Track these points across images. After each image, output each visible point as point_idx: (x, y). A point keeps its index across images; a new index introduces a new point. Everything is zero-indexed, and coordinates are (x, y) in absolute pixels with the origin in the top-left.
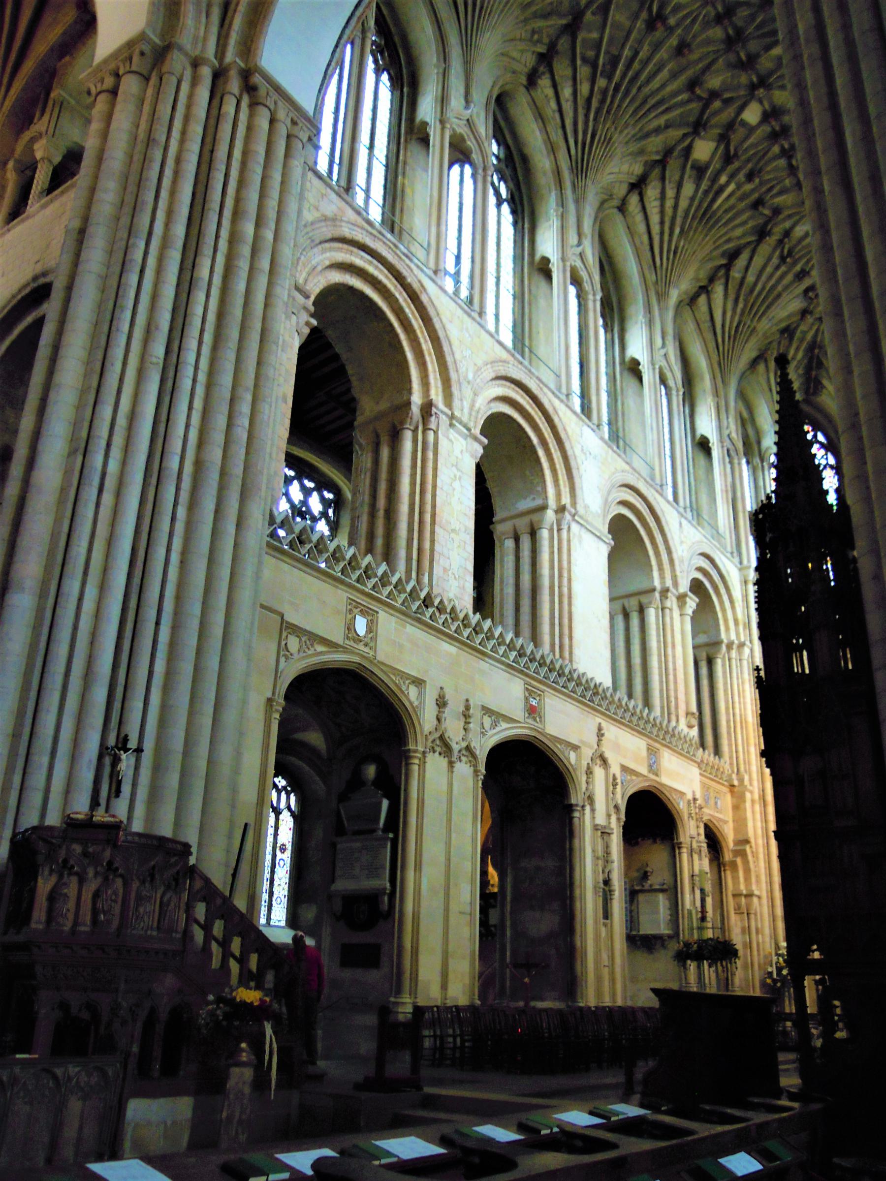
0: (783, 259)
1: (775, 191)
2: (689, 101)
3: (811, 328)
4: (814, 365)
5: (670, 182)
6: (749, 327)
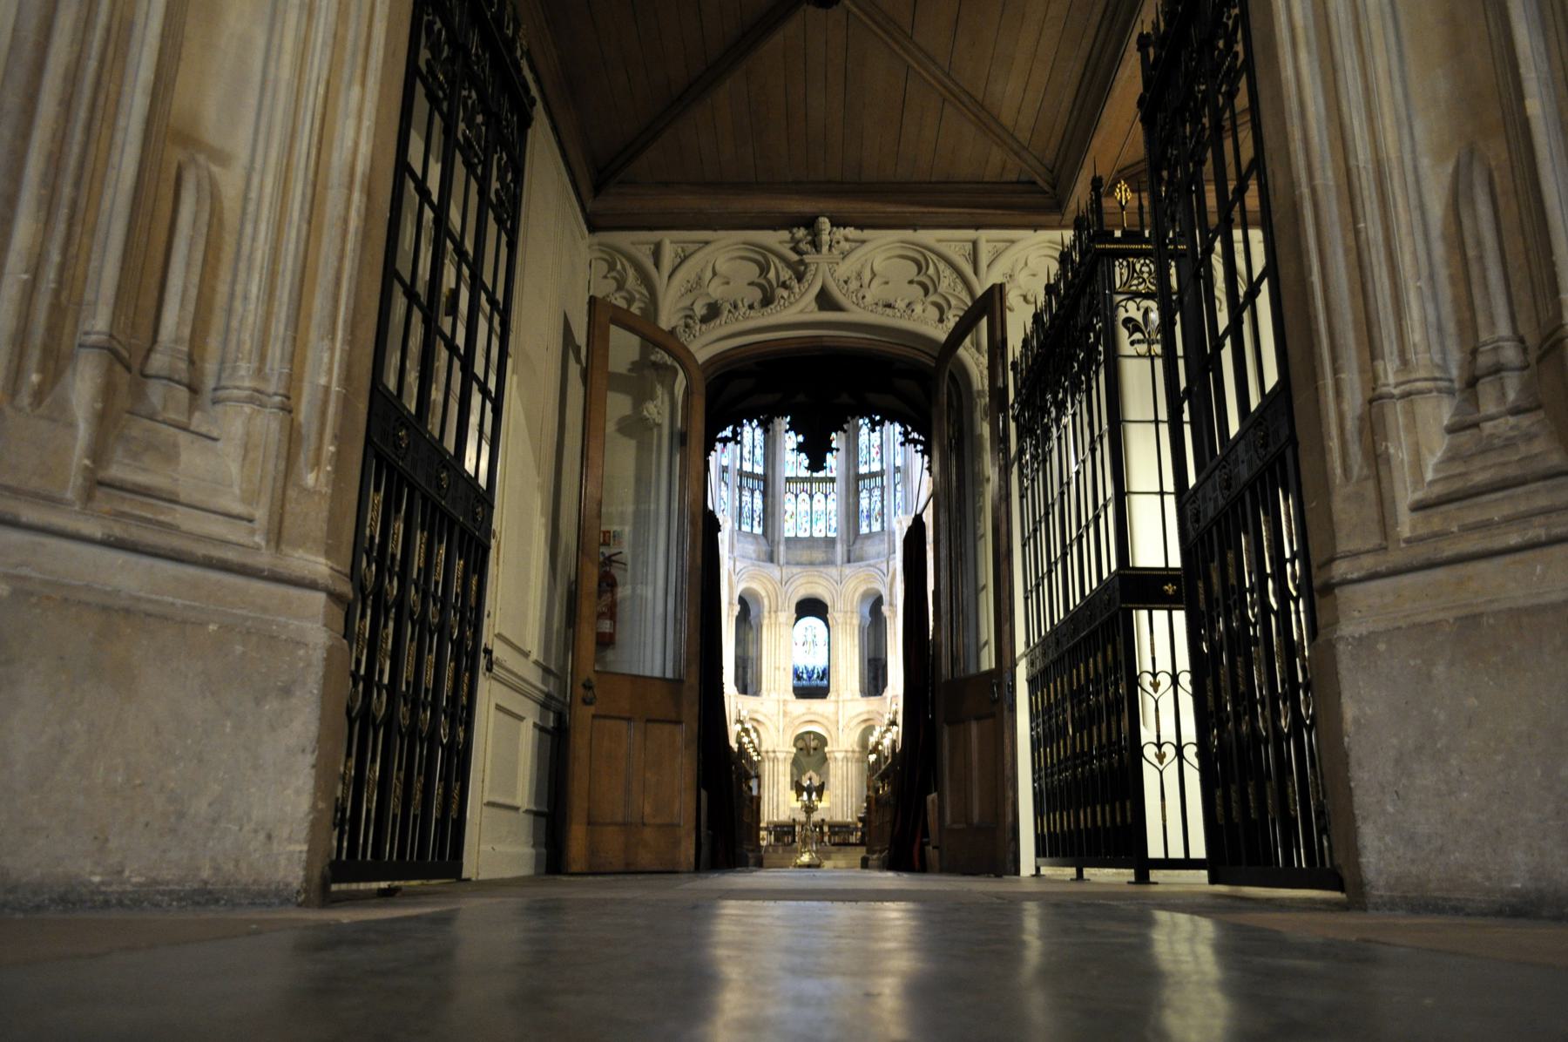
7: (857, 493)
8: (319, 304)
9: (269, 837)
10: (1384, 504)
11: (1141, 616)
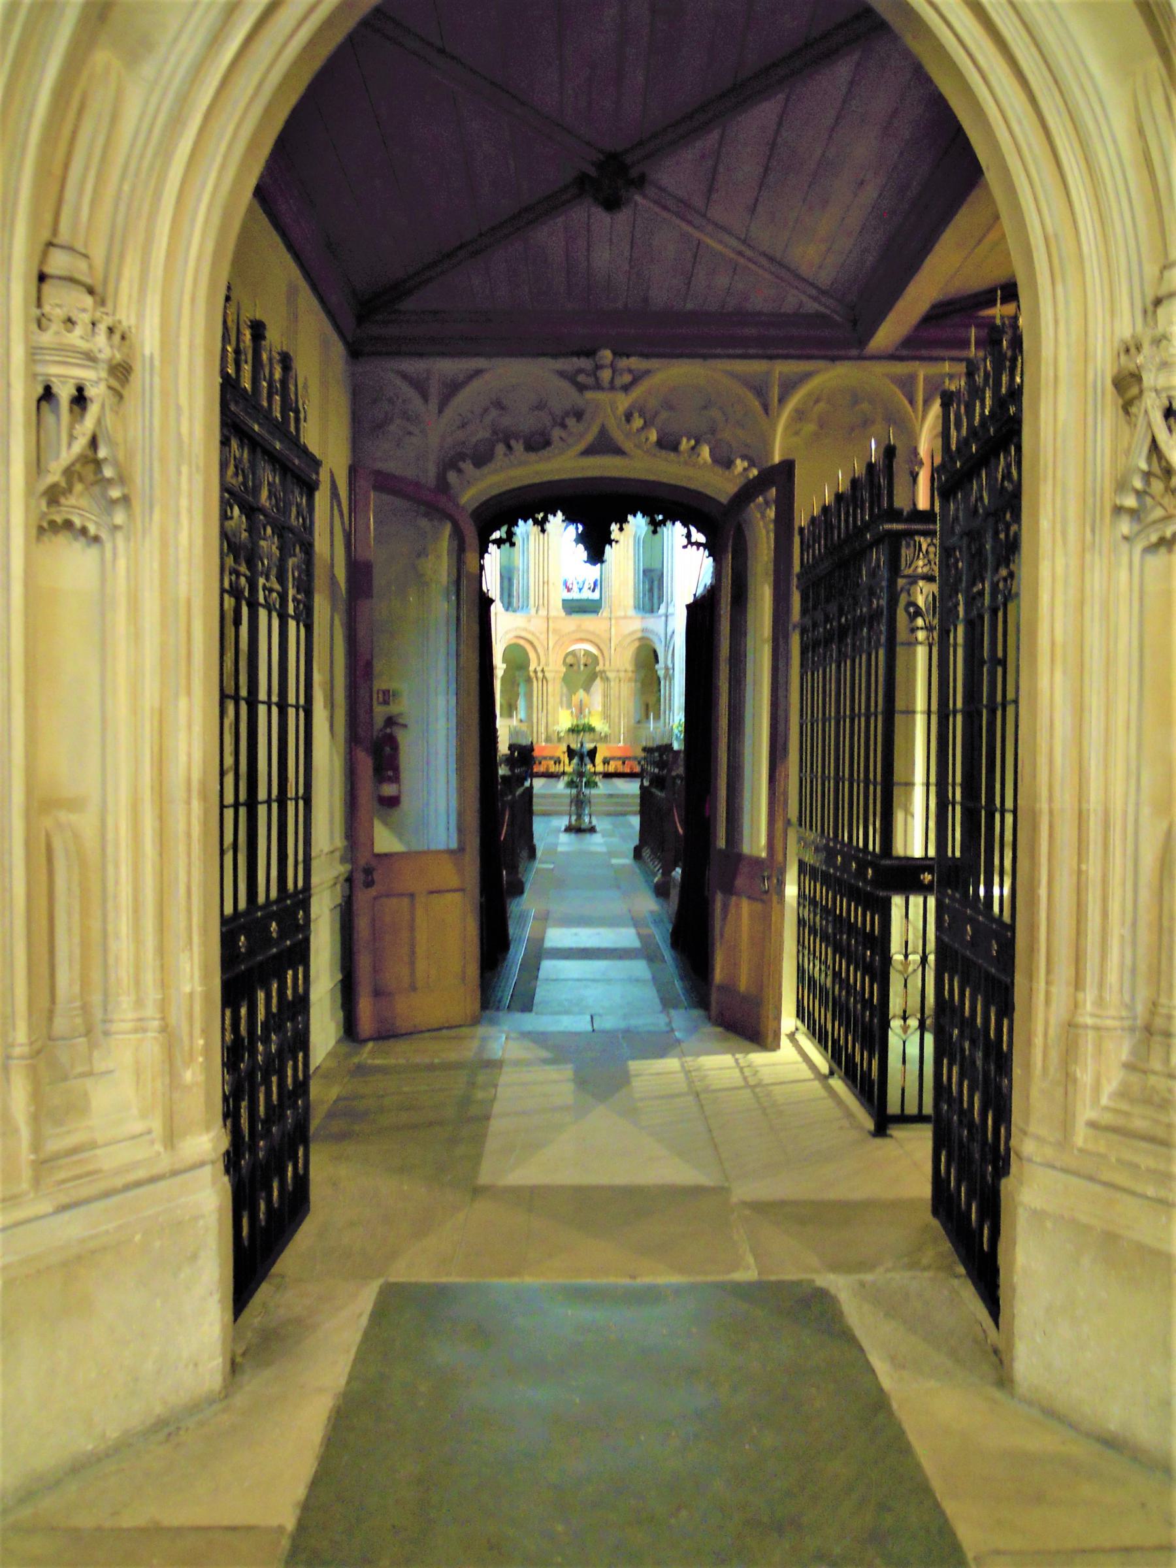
8: (177, 919)
9: (196, 1365)
10: (1066, 1125)
11: (897, 901)
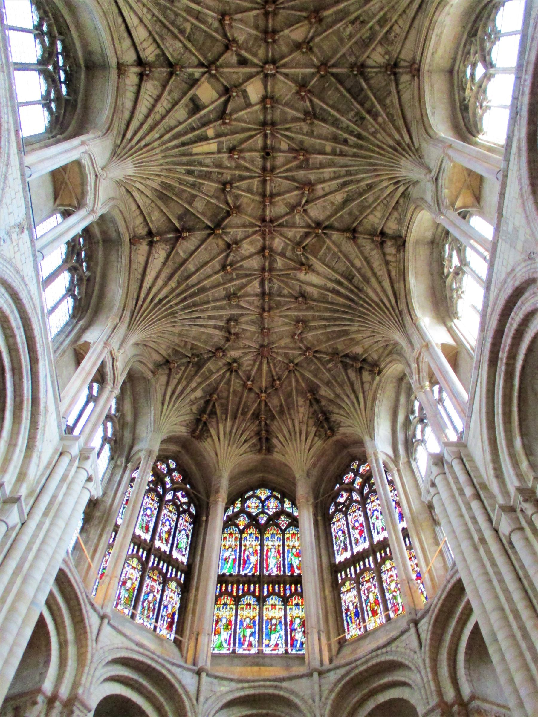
0: (224, 267)
1: (243, 184)
2: (216, 31)
3: (218, 371)
4: (208, 412)
5: (169, 94)
6: (171, 307)
7: (336, 587)
